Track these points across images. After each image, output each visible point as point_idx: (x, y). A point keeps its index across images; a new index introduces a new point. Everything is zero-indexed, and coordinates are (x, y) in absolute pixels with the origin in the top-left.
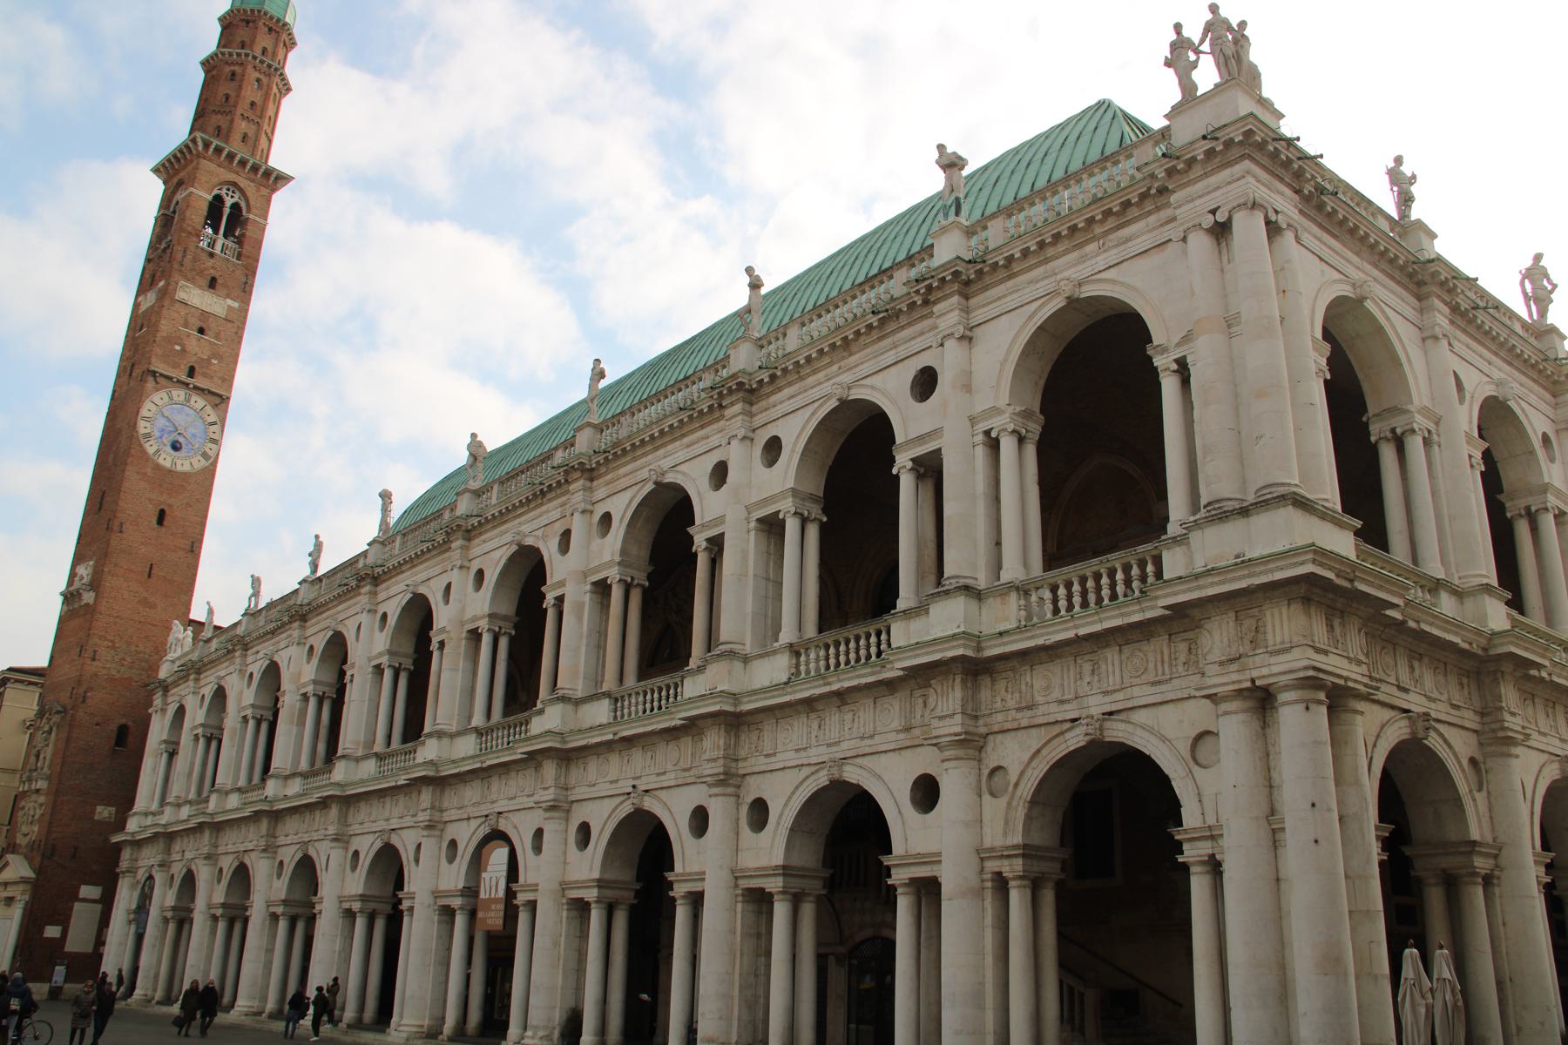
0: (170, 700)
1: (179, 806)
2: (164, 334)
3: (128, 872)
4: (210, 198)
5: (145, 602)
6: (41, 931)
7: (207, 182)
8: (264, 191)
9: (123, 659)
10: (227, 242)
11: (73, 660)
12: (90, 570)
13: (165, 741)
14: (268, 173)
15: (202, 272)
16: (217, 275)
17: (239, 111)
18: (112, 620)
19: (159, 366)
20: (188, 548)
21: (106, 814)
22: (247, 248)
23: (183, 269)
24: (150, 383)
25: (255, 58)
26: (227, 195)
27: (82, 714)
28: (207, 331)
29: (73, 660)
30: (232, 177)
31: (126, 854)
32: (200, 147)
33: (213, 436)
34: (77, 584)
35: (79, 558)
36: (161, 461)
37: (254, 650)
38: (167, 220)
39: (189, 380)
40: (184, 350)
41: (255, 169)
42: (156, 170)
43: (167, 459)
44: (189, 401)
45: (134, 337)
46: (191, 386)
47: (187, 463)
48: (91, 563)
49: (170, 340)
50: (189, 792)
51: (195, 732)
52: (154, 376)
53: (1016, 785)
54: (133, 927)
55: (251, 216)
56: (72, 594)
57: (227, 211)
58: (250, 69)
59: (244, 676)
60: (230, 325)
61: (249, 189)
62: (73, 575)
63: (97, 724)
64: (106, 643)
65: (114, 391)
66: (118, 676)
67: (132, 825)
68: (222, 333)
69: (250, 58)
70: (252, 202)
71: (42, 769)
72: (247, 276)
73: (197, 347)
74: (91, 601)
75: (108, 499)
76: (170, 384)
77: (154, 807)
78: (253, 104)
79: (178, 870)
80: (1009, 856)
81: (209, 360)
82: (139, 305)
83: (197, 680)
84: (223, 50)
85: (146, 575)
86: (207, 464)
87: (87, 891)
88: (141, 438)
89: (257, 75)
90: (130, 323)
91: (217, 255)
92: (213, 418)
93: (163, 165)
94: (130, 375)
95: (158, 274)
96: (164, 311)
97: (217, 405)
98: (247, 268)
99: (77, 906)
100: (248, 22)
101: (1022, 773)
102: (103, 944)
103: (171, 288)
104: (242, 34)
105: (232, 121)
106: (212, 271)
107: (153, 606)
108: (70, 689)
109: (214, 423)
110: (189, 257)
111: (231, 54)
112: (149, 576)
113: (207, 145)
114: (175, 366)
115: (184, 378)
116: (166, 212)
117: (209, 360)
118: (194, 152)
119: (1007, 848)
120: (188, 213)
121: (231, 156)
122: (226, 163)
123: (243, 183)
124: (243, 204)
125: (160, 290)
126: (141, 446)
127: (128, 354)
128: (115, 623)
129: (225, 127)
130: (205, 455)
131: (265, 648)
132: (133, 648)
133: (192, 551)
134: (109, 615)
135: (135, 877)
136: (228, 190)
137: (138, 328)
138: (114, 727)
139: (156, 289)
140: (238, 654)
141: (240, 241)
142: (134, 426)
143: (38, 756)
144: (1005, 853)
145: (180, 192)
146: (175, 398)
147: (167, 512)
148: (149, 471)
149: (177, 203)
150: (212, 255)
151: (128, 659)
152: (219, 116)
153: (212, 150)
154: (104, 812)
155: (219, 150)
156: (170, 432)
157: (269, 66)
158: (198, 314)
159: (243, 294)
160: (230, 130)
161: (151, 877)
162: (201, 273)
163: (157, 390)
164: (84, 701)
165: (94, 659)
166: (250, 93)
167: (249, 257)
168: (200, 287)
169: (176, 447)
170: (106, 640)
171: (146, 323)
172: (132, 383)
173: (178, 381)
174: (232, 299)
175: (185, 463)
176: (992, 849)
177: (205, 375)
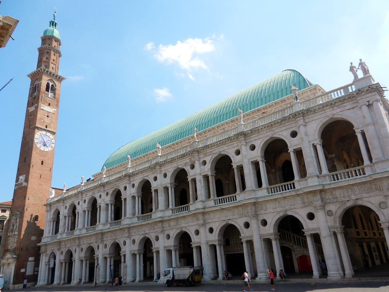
0: (52, 208)
1: (62, 234)
3: (44, 252)
5: (40, 184)
12: (24, 177)
14: (59, 78)
16: (50, 103)
19: (38, 125)
20: (50, 170)
21: (34, 238)
22: (56, 96)
24: (36, 130)
25: (53, 48)
29: (22, 200)
31: (43, 249)
32: (43, 71)
33: (53, 142)
35: (18, 175)
36: (41, 149)
39: (46, 129)
40: (44, 121)
42: (29, 76)
43: (42, 148)
47: (47, 149)
49: (40, 119)
50: (65, 230)
57: (50, 87)
58: (52, 51)
67: (44, 240)
69: (52, 48)
73: (47, 121)
74: (26, 185)
77: (51, 235)
78: (54, 60)
79: (65, 250)
83: (63, 202)
85: (40, 177)
86: (52, 149)
87: (31, 259)
92: (52, 138)
93: (31, 75)
94: (29, 128)
96: (38, 112)
99: (28, 263)
100: (50, 39)
102: (38, 271)
103: (39, 106)
104: (48, 42)
105: (49, 64)
110: (43, 98)
111: (46, 47)
113: (44, 70)
116: (33, 87)
120: (41, 87)
121: (50, 73)
125: (36, 106)
126: (36, 145)
130: (52, 147)
135: (46, 253)
141: (55, 94)
145: (37, 81)
152: (46, 63)
154: (33, 238)
155: (47, 72)
157: (57, 50)
161: (53, 253)
162: (46, 102)
164: (27, 210)
166: (53, 57)
167: (57, 98)
172: (30, 130)
173: (44, 129)
175: (46, 149)
177: (50, 127)
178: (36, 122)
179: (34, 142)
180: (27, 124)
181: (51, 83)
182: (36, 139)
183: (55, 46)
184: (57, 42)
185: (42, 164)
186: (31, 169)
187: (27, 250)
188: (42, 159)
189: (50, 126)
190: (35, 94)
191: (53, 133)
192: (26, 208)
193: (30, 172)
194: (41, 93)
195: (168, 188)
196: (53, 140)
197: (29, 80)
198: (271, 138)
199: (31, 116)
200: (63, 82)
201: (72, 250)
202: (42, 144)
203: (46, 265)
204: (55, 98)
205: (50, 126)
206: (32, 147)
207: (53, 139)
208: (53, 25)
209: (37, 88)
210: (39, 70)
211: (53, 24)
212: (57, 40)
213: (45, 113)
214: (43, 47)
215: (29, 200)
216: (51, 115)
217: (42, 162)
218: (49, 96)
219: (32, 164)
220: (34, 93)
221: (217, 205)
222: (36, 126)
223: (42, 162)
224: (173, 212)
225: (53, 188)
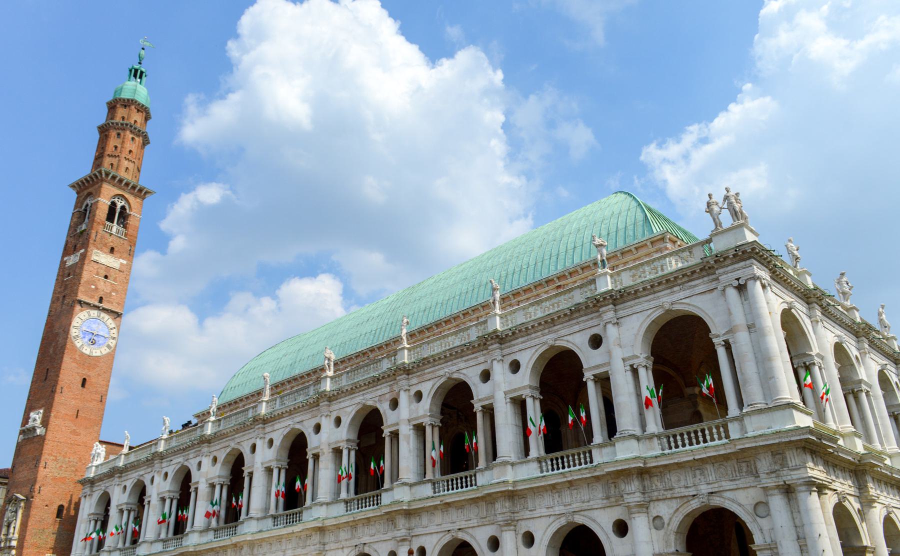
2: (85, 280)
4: (109, 203)
8: (138, 200)
9: (61, 466)
10: (119, 228)
11: (30, 469)
12: (41, 415)
13: (93, 514)
14: (140, 190)
15: (106, 244)
16: (114, 246)
17: (123, 155)
18: (55, 444)
19: (82, 297)
22: (130, 231)
23: (95, 243)
24: (78, 307)
27: (38, 500)
28: (109, 277)
32: (104, 176)
33: (113, 335)
34: (30, 424)
35: (29, 408)
36: (84, 351)
38: (83, 214)
39: (100, 305)
40: (97, 288)
41: (134, 187)
42: (73, 186)
43: (87, 350)
44: (99, 316)
45: (63, 281)
46: (101, 308)
48: (41, 411)
49: (89, 283)
50: (118, 543)
51: (120, 508)
55: (132, 213)
56: (28, 430)
57: (118, 210)
59: (161, 474)
60: (121, 273)
62: (26, 419)
63: (46, 506)
65: (50, 311)
66: (58, 476)
68: (118, 279)
70: (132, 205)
71: (14, 534)
72: (131, 246)
73: (104, 287)
74: (43, 433)
75: (51, 374)
78: (130, 151)
81: (110, 293)
82: (66, 262)
84: (112, 121)
85: (75, 416)
88: (72, 338)
89: (131, 136)
90: (59, 272)
92: (113, 325)
93: (78, 184)
95: (78, 246)
96: (85, 267)
98: (131, 242)
103: (89, 253)
105: (119, 161)
108: (30, 486)
109: (114, 328)
110: (99, 236)
112: (77, 417)
113: (107, 174)
114: (92, 297)
115: (97, 303)
117: (110, 293)
118: (99, 178)
120: (97, 212)
121: (121, 181)
122: (118, 184)
123: (127, 196)
124: (127, 207)
127: (59, 290)
128: (57, 446)
129: (115, 164)
130: (109, 347)
131: (179, 460)
132: (67, 459)
133: (101, 401)
134: (53, 441)
137: (66, 275)
138: (56, 507)
139: (78, 254)
141: (125, 227)
142: (67, 332)
143: (9, 526)
145: (88, 199)
146: (92, 315)
147: (87, 380)
149: (87, 205)
150: (111, 234)
151: (64, 466)
153: (110, 177)
159: (128, 256)
160: (118, 166)
162: (105, 245)
164: (39, 493)
165: (45, 468)
168: (105, 253)
170: (52, 455)
171: (72, 273)
172: (64, 308)
174: (123, 259)
175: (97, 352)
177: (109, 302)
178: (77, 289)
179: (69, 336)
180: (59, 292)
182: (74, 327)
183: (135, 121)
184: (142, 112)
185: (83, 385)
186: (57, 397)
188: (85, 373)
189: (108, 299)
190: (84, 227)
191: (117, 315)
192: (37, 487)
193: (54, 404)
194: (95, 224)
195: (425, 427)
197: (73, 195)
198: (668, 311)
199: (69, 275)
200: (149, 198)
202: (86, 340)
204: (126, 235)
205: (108, 299)
206: (63, 347)
207: (112, 329)
208: (135, 76)
209: (88, 212)
210: (95, 175)
211: (137, 74)
212: (143, 110)
213: (99, 270)
214: (109, 124)
215: (47, 470)
216: (113, 274)
217: (84, 380)
218: (114, 230)
219: (61, 383)
220: (81, 224)
221: (545, 474)
222: (78, 298)
223: (84, 380)
224: (434, 489)
225: (101, 442)
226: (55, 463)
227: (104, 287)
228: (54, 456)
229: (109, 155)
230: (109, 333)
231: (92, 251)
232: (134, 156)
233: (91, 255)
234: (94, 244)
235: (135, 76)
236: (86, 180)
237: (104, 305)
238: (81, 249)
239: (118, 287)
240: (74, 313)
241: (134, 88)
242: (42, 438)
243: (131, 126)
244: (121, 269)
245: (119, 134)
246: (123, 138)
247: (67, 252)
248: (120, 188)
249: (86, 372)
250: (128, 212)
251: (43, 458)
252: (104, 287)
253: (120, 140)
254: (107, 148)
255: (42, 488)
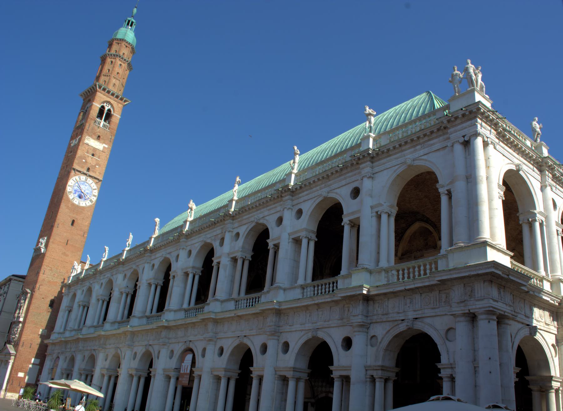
3: (50, 354)
4: (100, 106)
6: (17, 374)
7: (99, 101)
10: (105, 123)
12: (45, 240)
17: (113, 75)
18: (52, 259)
23: (88, 132)
24: (73, 173)
26: (106, 106)
30: (108, 99)
36: (74, 202)
37: (104, 274)
39: (88, 173)
40: (86, 162)
43: (77, 201)
46: (88, 175)
48: (46, 238)
49: (82, 158)
51: (79, 304)
52: (75, 171)
53: (380, 343)
54: (50, 375)
55: (115, 114)
60: (104, 153)
61: (114, 104)
63: (43, 298)
64: (49, 268)
68: (101, 157)
70: (115, 109)
73: (91, 161)
76: (80, 173)
77: (62, 331)
78: (118, 73)
80: (376, 370)
85: (66, 244)
89: (120, 63)
91: (101, 127)
95: (78, 133)
96: (80, 147)
97: (97, 183)
101: (383, 338)
103: (83, 138)
105: (110, 79)
106: (99, 133)
107: (67, 256)
109: (95, 189)
110: (90, 128)
112: (67, 244)
114: (83, 167)
115: (85, 172)
117: (95, 166)
118: (95, 89)
119: (376, 366)
120: (91, 112)
123: (112, 102)
126: (67, 196)
129: (107, 81)
130: (91, 201)
131: (108, 275)
134: (50, 258)
136: (107, 104)
140: (97, 275)
141: (109, 123)
142: (65, 188)
144: (375, 368)
145: (89, 104)
146: (82, 179)
148: (70, 206)
150: (99, 127)
156: (79, 191)
158: (92, 149)
162: (94, 134)
163: (75, 176)
164: (39, 289)
168: (94, 139)
169: (80, 197)
170: (49, 266)
174: (105, 144)
176: (370, 366)
177: (93, 171)
179: (65, 191)
181: (106, 107)
182: (69, 186)
183: (124, 54)
185: (73, 224)
187: (30, 347)
188: (74, 216)
192: (38, 285)
194: (89, 119)
196: (95, 191)
199: (71, 152)
201: (75, 356)
202: (76, 195)
203: (49, 374)
215: (45, 275)
217: (73, 222)
223: (73, 222)
226: (51, 272)
227: (91, 161)
228: (50, 268)
229: (104, 75)
230: (92, 192)
231: (85, 137)
232: (120, 77)
233: (84, 139)
234: (87, 133)
235: (128, 24)
236: (88, 91)
237: (91, 173)
238: (79, 136)
239: (101, 162)
240: (70, 176)
241: (126, 32)
242: (44, 254)
243: (120, 57)
244: (104, 151)
245: (112, 62)
246: (114, 65)
247: (72, 138)
248: (108, 97)
249: (74, 216)
250: (112, 113)
251: (43, 268)
252: (91, 161)
253: (112, 66)
254: (103, 70)
255: (40, 287)
